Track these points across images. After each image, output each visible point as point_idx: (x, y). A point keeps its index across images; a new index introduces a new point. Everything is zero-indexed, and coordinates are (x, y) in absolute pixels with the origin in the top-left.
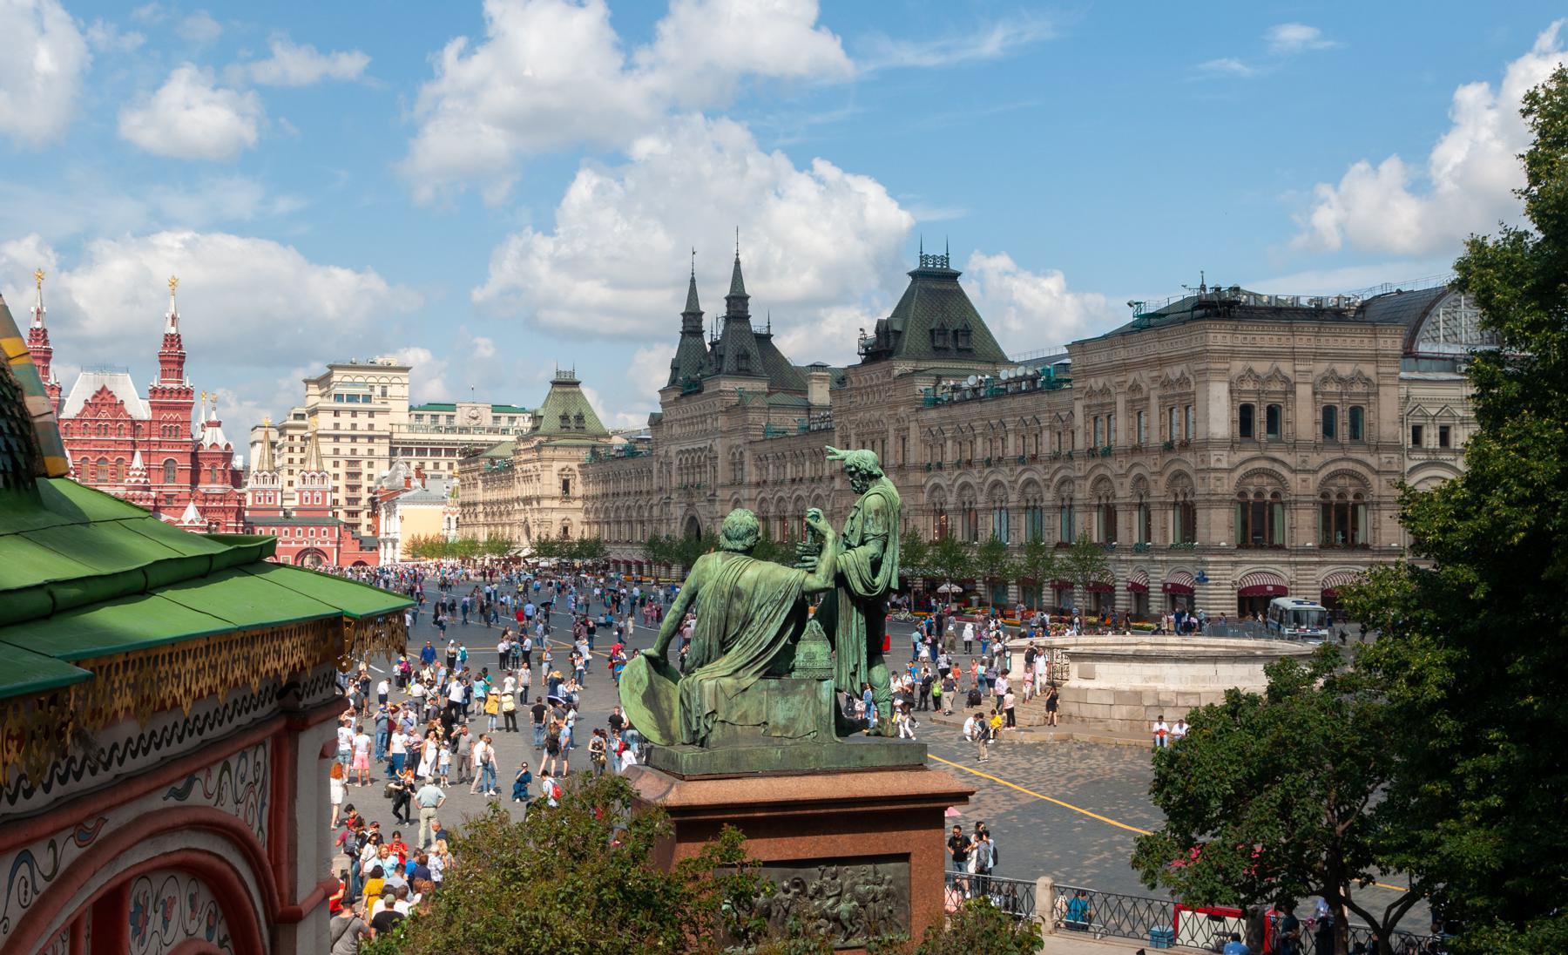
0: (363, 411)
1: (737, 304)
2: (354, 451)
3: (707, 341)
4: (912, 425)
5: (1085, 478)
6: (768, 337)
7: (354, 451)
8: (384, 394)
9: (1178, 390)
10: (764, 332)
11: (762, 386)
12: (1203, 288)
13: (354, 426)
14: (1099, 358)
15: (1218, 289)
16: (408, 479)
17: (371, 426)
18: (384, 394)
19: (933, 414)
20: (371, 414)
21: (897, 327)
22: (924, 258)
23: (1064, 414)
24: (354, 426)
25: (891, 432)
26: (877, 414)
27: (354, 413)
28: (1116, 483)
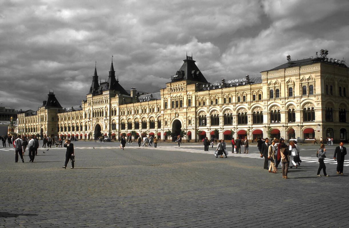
1: (112, 73)
3: (99, 82)
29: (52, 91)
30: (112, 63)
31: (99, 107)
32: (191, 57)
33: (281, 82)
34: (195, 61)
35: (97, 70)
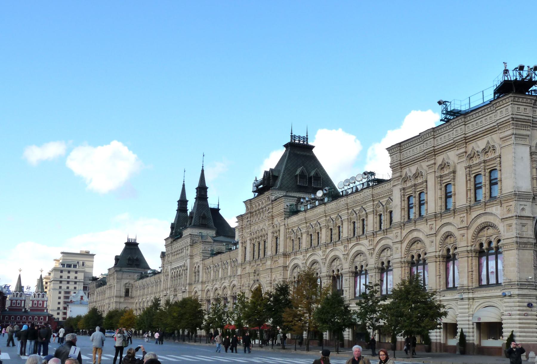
0: (73, 271)
1: (202, 191)
2: (68, 288)
4: (282, 229)
5: (401, 242)
6: (218, 210)
7: (68, 288)
8: (83, 265)
9: (482, 158)
10: (216, 207)
11: (212, 233)
12: (506, 71)
13: (68, 277)
14: (409, 154)
15: (521, 68)
16: (82, 297)
17: (76, 278)
18: (83, 265)
19: (295, 219)
20: (76, 272)
21: (276, 174)
22: (293, 137)
23: (384, 201)
24: (68, 277)
25: (270, 235)
26: (261, 226)
27: (69, 272)
28: (427, 241)
29: (132, 237)
30: (203, 171)
31: (178, 266)
32: (304, 138)
33: (427, 168)
34: (313, 147)
35: (185, 186)
